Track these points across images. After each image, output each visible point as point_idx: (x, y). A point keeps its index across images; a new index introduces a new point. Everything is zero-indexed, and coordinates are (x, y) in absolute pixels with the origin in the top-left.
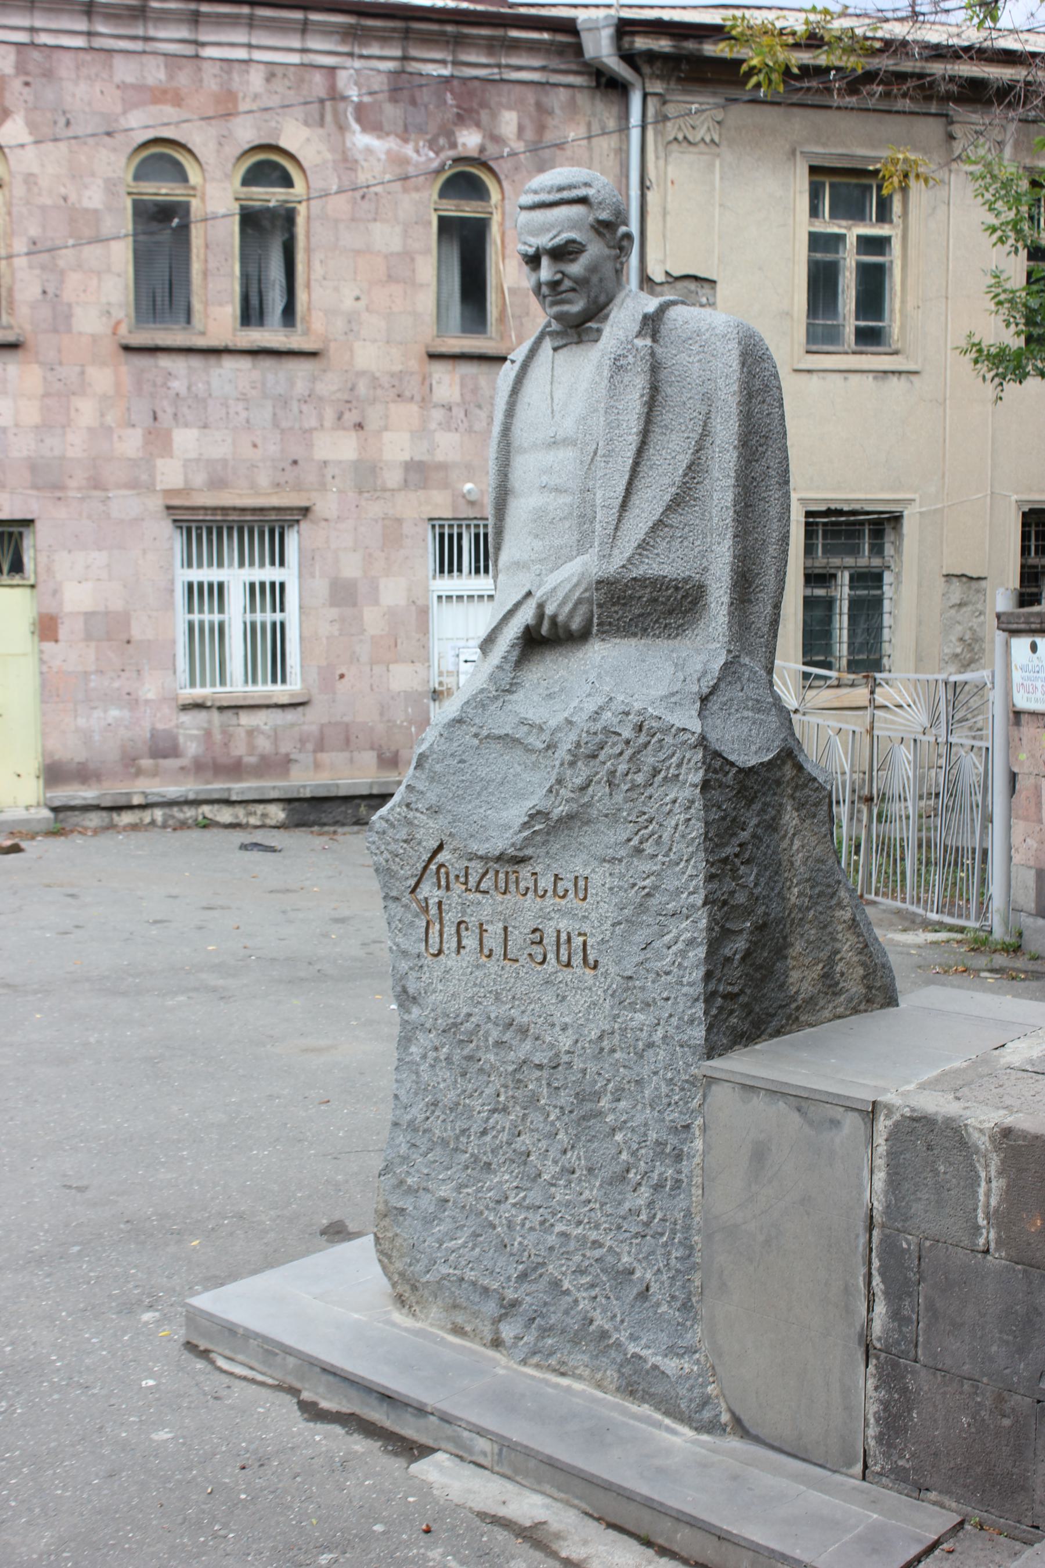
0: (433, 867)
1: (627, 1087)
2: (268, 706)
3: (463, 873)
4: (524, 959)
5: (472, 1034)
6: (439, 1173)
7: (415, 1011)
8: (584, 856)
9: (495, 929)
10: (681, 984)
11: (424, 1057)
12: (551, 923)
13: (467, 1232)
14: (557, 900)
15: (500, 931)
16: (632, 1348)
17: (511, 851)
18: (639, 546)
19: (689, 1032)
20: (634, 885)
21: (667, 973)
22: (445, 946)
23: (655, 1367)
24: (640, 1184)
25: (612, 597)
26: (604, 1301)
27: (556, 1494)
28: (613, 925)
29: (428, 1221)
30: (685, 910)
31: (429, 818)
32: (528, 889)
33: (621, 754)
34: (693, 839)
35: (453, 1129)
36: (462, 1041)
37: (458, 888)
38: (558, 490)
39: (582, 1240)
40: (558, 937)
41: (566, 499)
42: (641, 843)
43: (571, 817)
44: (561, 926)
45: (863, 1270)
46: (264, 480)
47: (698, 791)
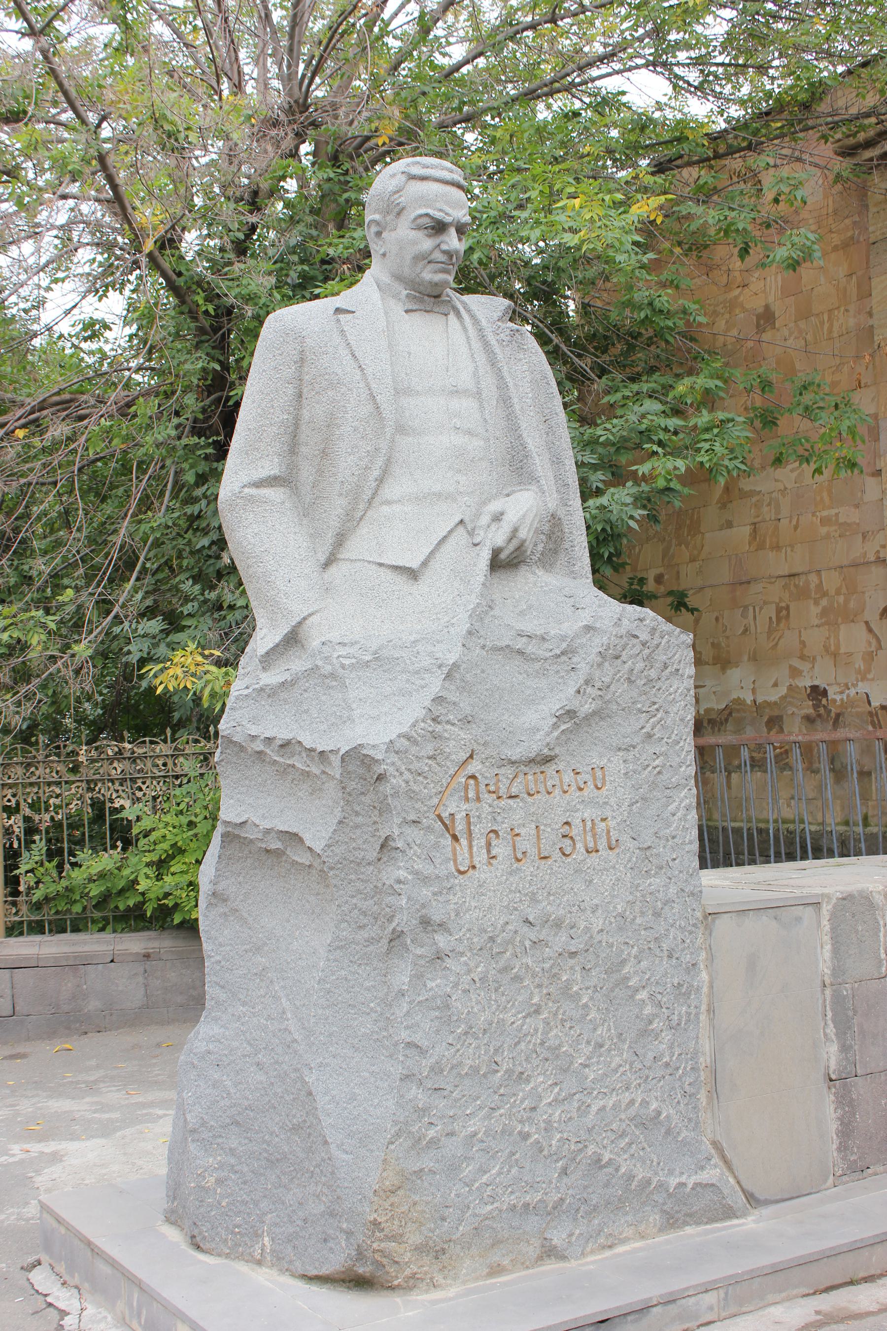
4: (557, 855)
6: (467, 1108)
9: (527, 831)
15: (534, 832)
16: (673, 1182)
20: (648, 766)
21: (673, 838)
23: (697, 1185)
26: (641, 1153)
27: (778, 1297)
29: (453, 1169)
30: (684, 781)
37: (488, 798)
40: (585, 826)
41: (477, 443)
43: (594, 713)
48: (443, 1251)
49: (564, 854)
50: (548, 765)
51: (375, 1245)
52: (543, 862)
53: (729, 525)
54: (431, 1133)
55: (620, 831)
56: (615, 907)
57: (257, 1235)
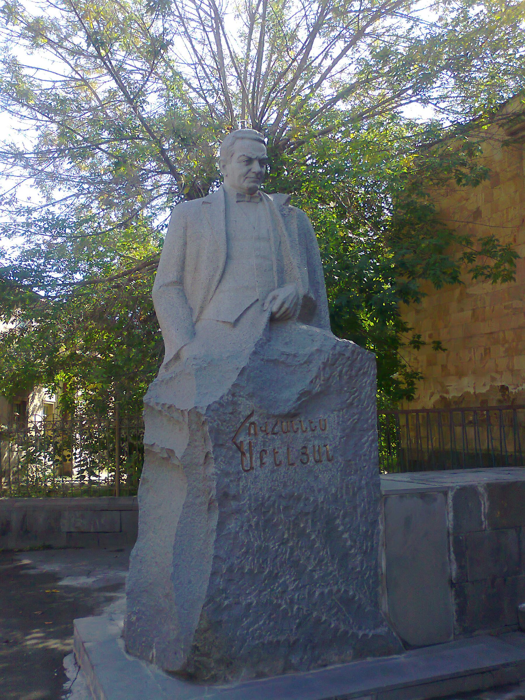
4: (298, 463)
10: (370, 459)
11: (242, 527)
13: (265, 616)
16: (361, 634)
17: (293, 411)
21: (365, 455)
22: (254, 464)
24: (356, 555)
28: (340, 438)
32: (298, 428)
37: (261, 434)
39: (330, 592)
43: (321, 392)
45: (448, 554)
48: (231, 663)
49: (303, 463)
51: (196, 658)
53: (462, 310)
54: (226, 603)
56: (331, 490)
57: (151, 648)
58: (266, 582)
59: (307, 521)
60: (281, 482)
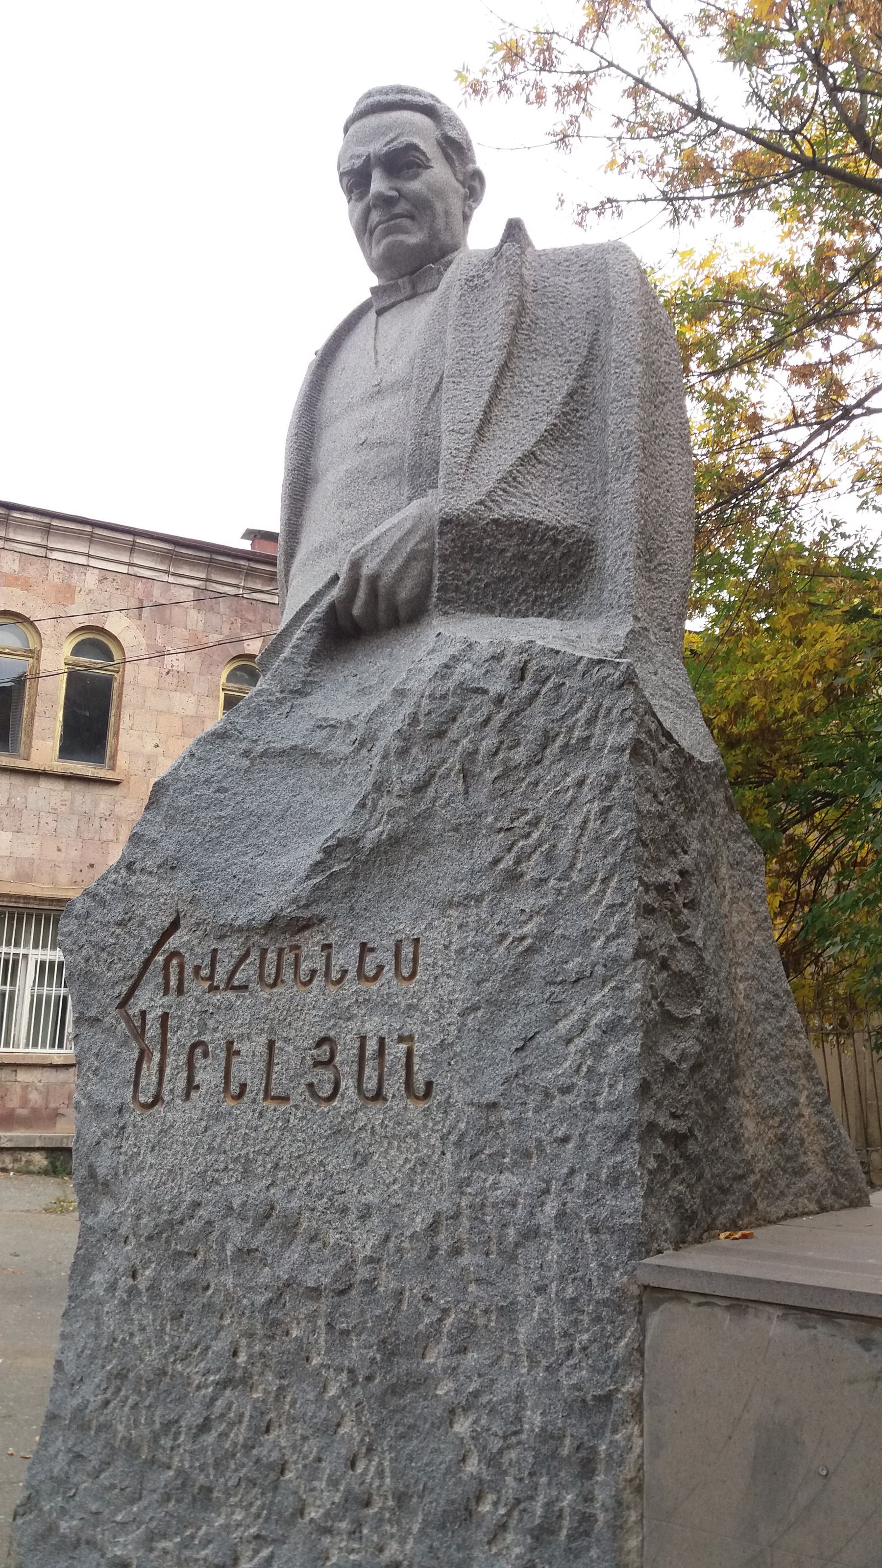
0: (160, 958)
1: (481, 1321)
2: (43, 1066)
3: (208, 960)
4: (299, 1094)
5: (197, 1240)
6: (118, 1510)
7: (106, 1206)
8: (412, 906)
9: (252, 1048)
10: (593, 1108)
11: (112, 1287)
12: (351, 1025)
14: (364, 986)
15: (262, 1050)
18: (503, 479)
19: (609, 1201)
20: (504, 936)
21: (566, 1090)
25: (463, 548)
28: (462, 1014)
30: (600, 970)
31: (161, 879)
32: (313, 972)
33: (486, 722)
34: (616, 842)
35: (151, 1422)
36: (179, 1254)
37: (196, 988)
38: (381, 444)
40: (362, 1048)
42: (518, 862)
43: (395, 841)
44: (369, 1027)
46: (63, 878)
47: (626, 757)
50: (307, 933)
52: (272, 1105)
55: (437, 1064)
58: (171, 1505)
59: (312, 1317)
60: (236, 1160)
